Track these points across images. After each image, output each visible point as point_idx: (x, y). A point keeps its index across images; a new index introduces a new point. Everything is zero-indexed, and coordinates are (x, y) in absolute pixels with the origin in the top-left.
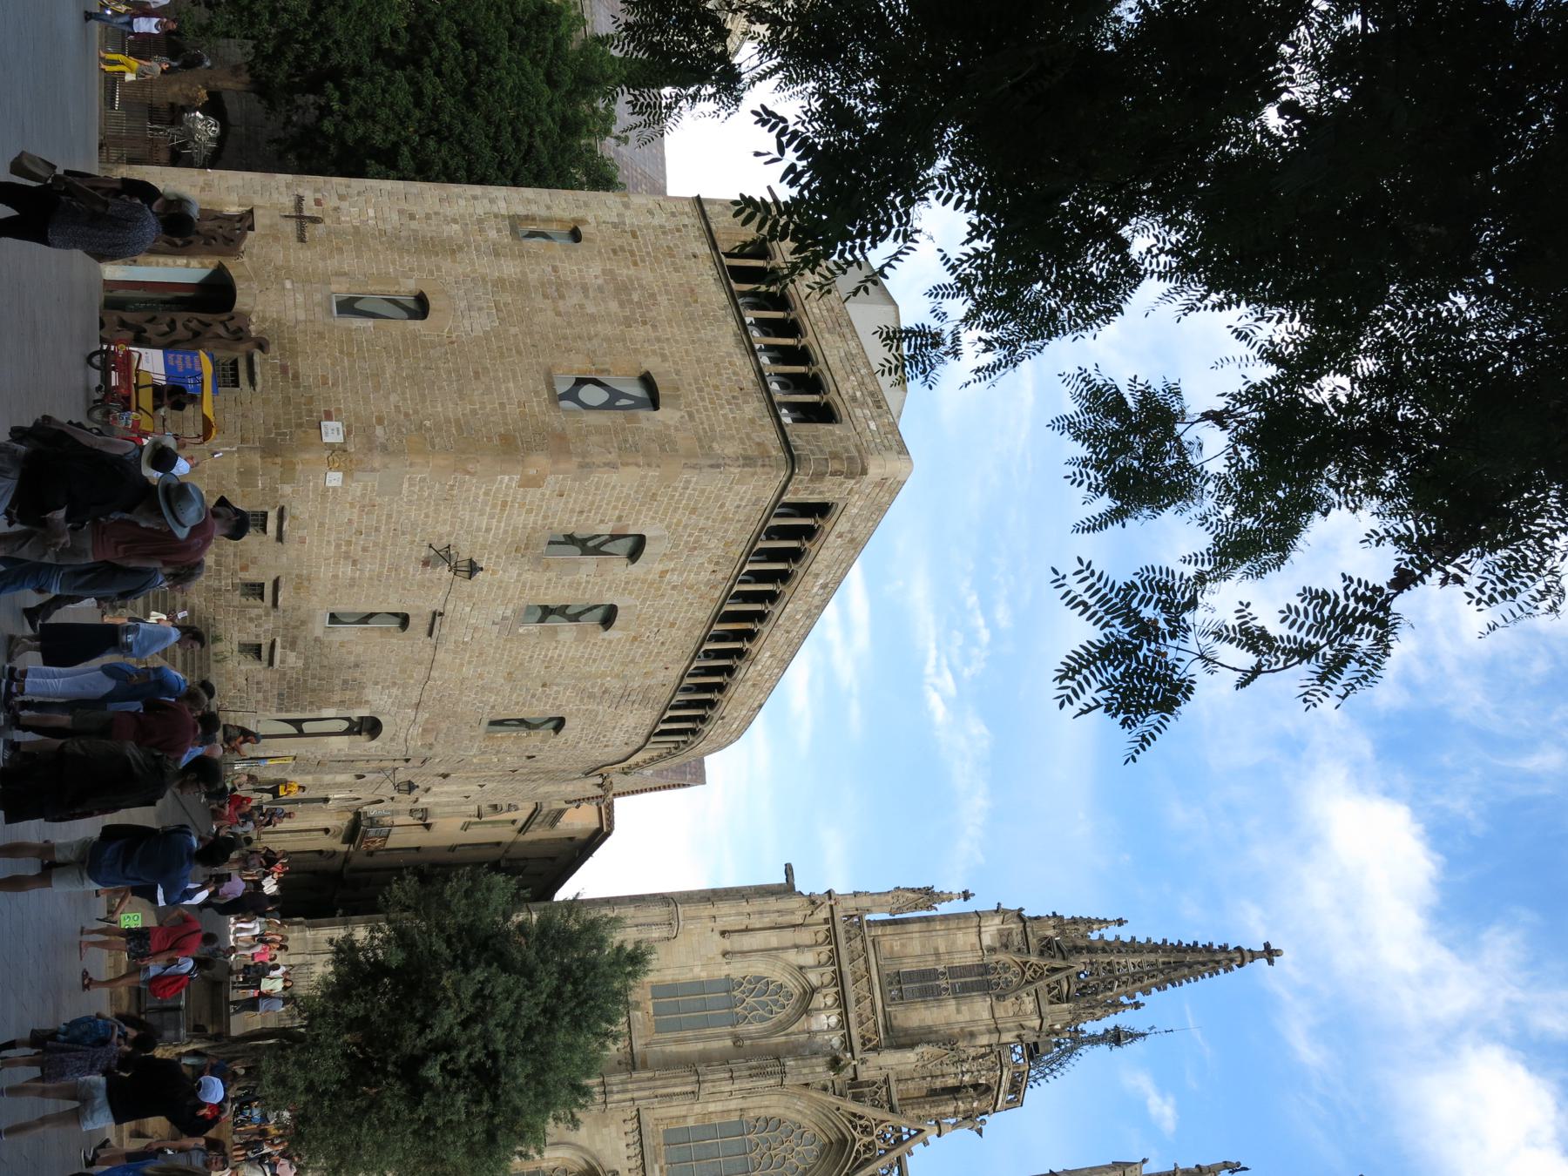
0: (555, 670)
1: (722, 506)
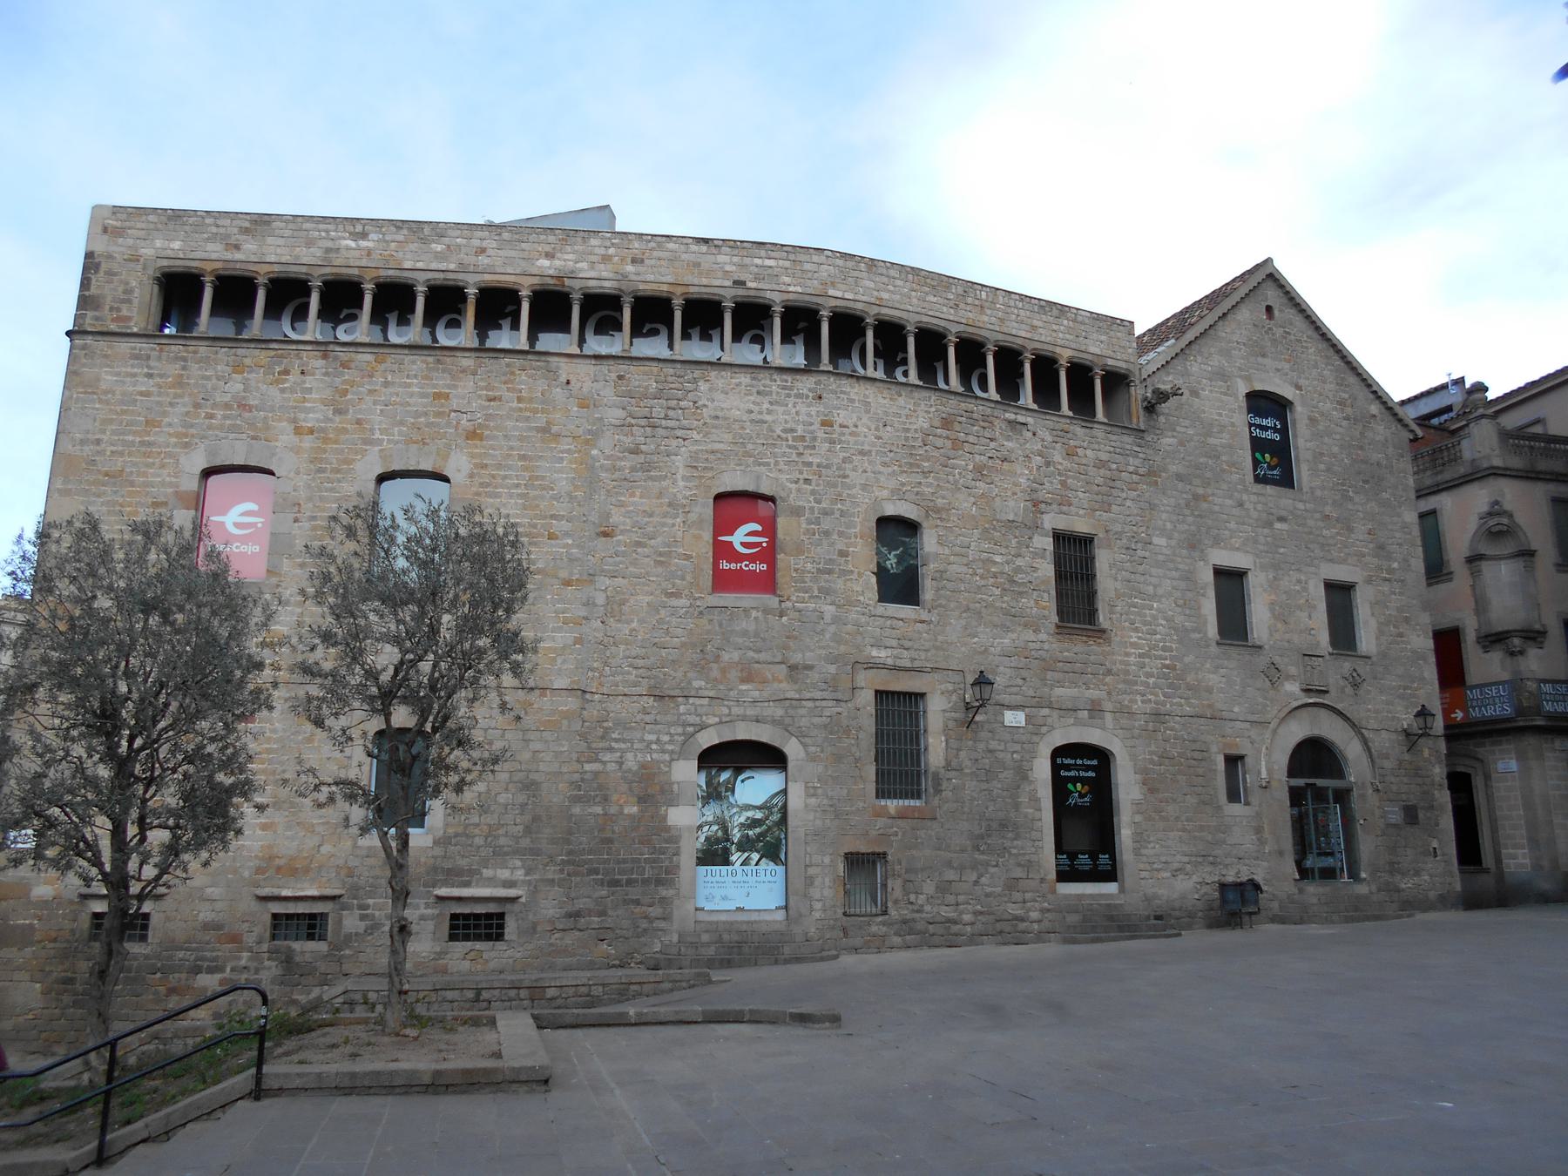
0: (560, 526)
1: (146, 394)
